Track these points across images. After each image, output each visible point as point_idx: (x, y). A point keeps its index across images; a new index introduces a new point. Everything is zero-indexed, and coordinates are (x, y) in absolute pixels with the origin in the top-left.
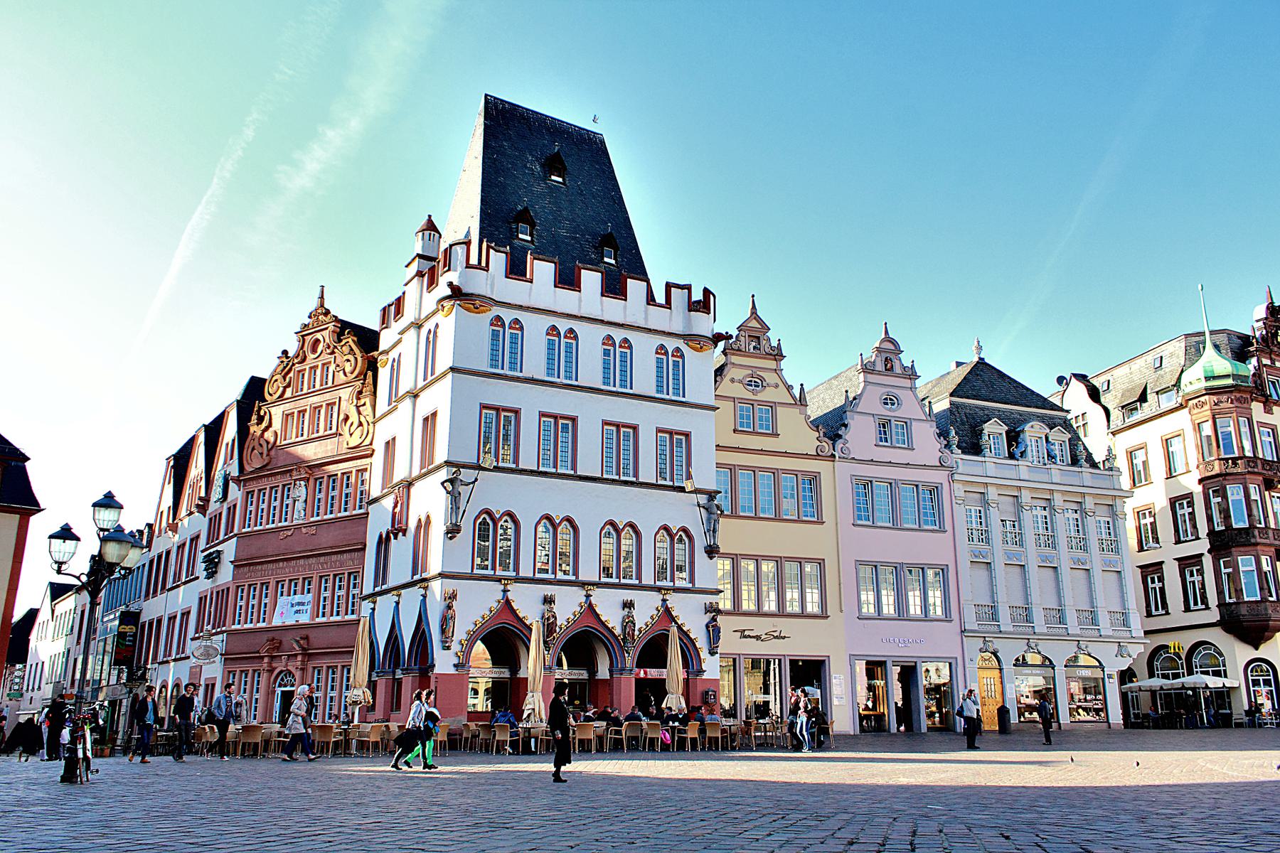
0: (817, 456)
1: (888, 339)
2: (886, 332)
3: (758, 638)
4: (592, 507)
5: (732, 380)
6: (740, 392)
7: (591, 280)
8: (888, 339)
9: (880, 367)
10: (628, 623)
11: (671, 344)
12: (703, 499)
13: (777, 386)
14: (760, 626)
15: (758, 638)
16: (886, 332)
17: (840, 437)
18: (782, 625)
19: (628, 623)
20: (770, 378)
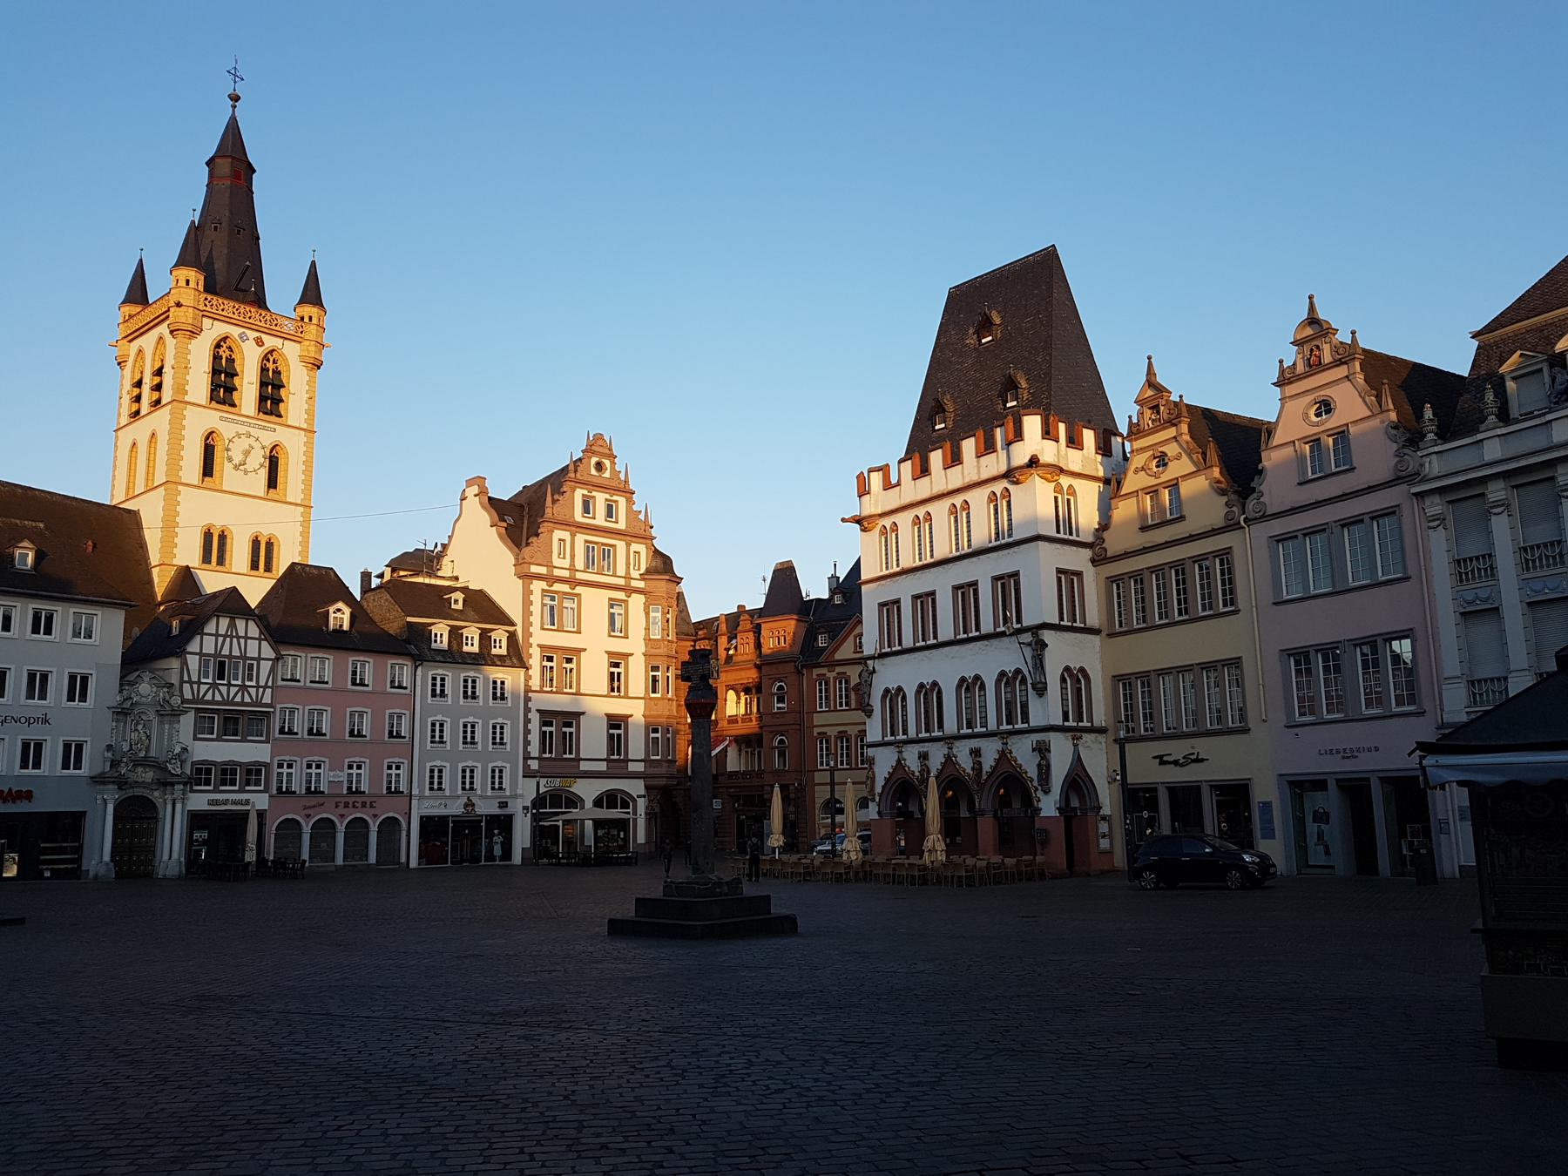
0: (1231, 526)
1: (1313, 320)
2: (1312, 308)
3: (1176, 763)
4: (946, 669)
5: (1136, 472)
6: (1145, 480)
7: (968, 446)
8: (1313, 320)
9: (1300, 368)
10: (978, 767)
11: (997, 488)
12: (1027, 638)
13: (1178, 457)
14: (1177, 749)
15: (1176, 763)
16: (1312, 308)
17: (1254, 490)
18: (1201, 746)
19: (978, 767)
20: (1171, 450)
